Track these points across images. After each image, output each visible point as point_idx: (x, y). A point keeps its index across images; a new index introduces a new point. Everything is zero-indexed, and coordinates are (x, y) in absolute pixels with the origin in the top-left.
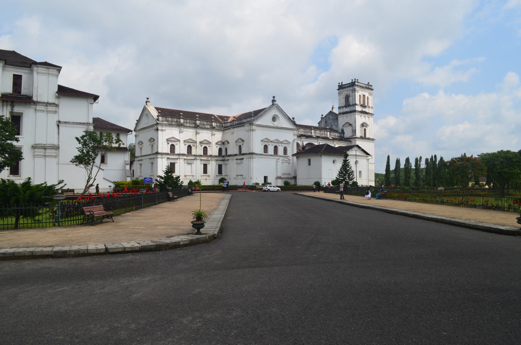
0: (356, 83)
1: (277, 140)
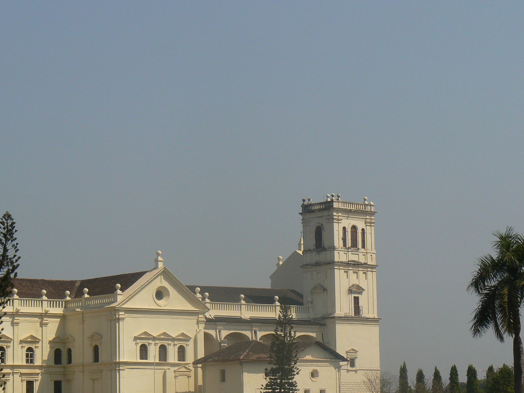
0: (335, 205)
1: (165, 334)
